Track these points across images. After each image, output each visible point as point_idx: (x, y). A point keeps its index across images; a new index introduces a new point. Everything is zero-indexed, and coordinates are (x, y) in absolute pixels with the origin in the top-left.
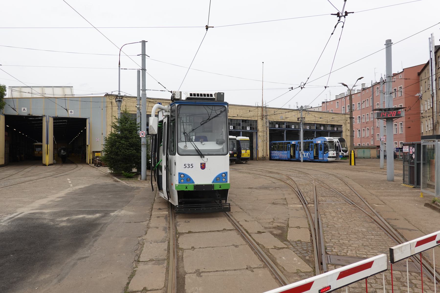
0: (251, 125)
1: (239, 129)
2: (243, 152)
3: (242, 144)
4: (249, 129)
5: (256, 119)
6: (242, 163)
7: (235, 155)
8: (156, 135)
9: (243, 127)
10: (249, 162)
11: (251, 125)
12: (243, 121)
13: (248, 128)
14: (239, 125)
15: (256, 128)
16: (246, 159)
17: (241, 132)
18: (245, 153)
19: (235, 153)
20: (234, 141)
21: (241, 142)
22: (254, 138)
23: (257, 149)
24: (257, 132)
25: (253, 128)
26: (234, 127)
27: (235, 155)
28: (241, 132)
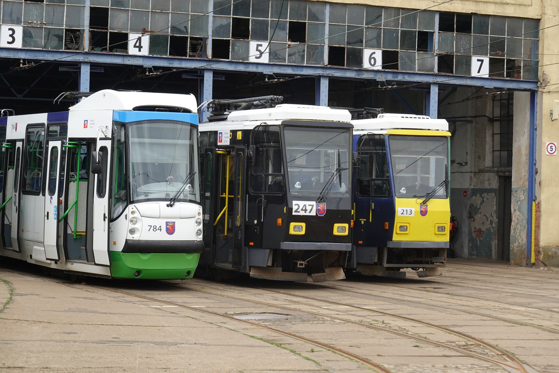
0: (497, 46)
1: (420, 67)
2: (405, 207)
3: (399, 164)
4: (485, 72)
5: (532, 13)
6: (402, 280)
7: (341, 229)
8: (326, 267)
9: (446, 63)
10: (446, 271)
11: (497, 46)
12: (449, 21)
13: (480, 68)
14: (424, 41)
15: (534, 68)
16: (423, 258)
17: (434, 91)
18: (422, 219)
19: (342, 217)
20: (343, 137)
21: (392, 145)
22: (516, 129)
23: (532, 197)
24: (533, 94)
25: (513, 69)
26: (390, 59)
27: (341, 229)
28: (434, 91)
